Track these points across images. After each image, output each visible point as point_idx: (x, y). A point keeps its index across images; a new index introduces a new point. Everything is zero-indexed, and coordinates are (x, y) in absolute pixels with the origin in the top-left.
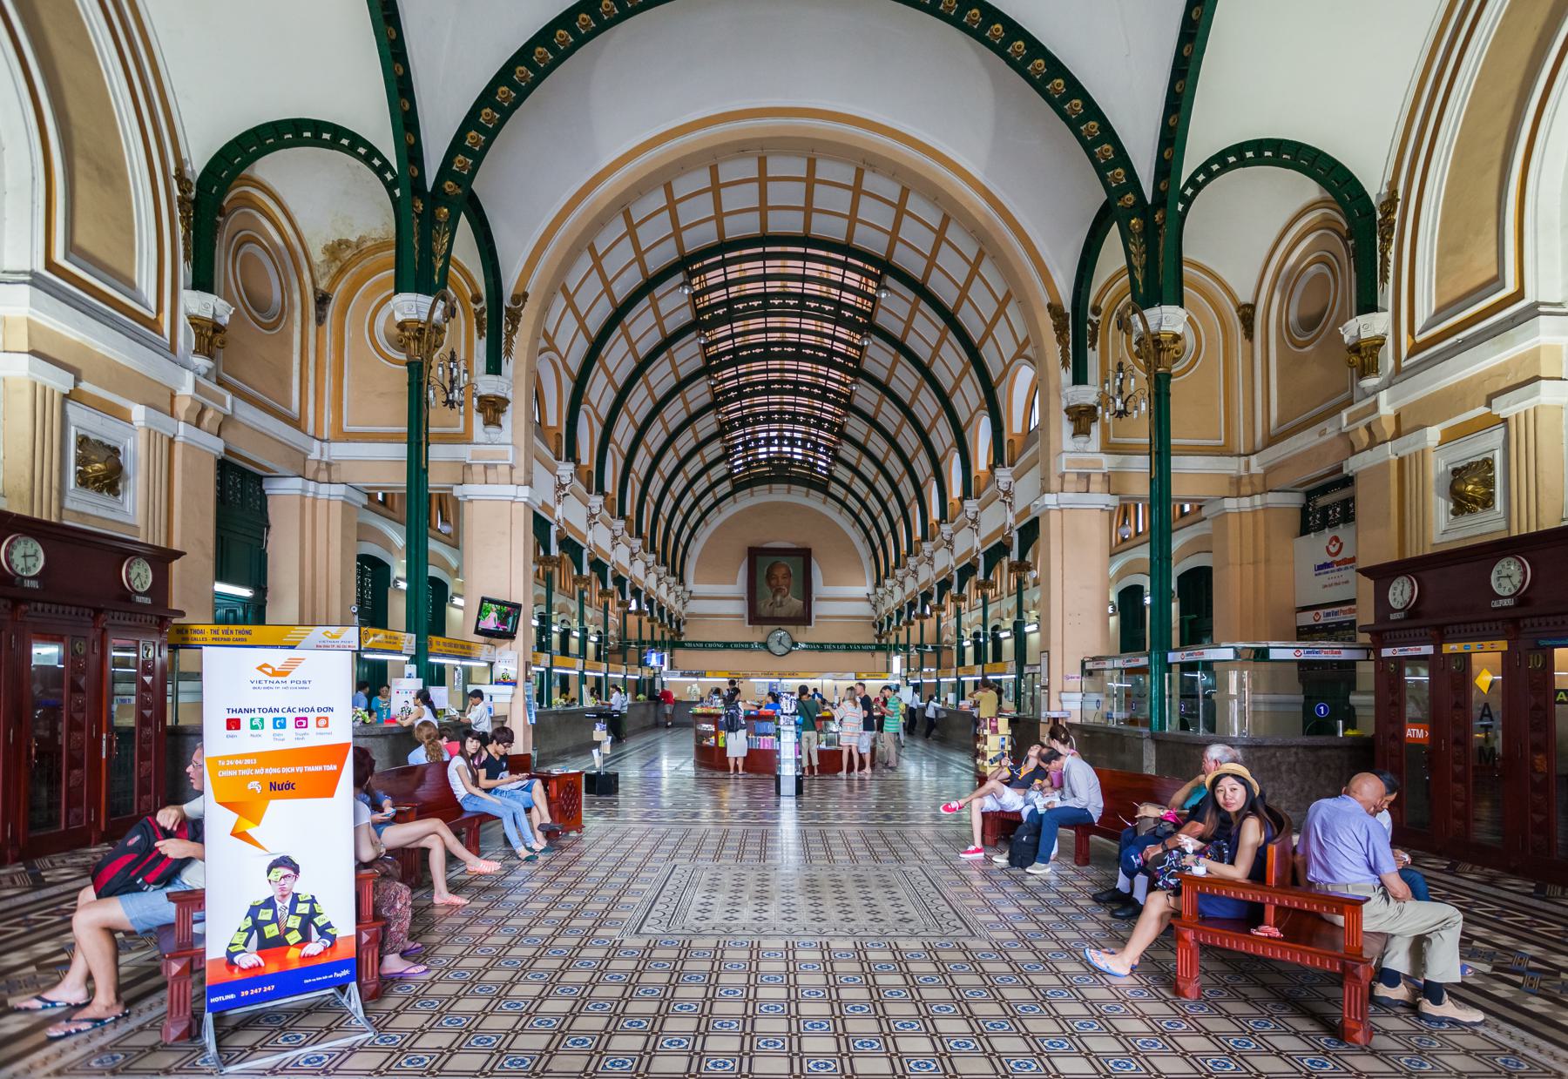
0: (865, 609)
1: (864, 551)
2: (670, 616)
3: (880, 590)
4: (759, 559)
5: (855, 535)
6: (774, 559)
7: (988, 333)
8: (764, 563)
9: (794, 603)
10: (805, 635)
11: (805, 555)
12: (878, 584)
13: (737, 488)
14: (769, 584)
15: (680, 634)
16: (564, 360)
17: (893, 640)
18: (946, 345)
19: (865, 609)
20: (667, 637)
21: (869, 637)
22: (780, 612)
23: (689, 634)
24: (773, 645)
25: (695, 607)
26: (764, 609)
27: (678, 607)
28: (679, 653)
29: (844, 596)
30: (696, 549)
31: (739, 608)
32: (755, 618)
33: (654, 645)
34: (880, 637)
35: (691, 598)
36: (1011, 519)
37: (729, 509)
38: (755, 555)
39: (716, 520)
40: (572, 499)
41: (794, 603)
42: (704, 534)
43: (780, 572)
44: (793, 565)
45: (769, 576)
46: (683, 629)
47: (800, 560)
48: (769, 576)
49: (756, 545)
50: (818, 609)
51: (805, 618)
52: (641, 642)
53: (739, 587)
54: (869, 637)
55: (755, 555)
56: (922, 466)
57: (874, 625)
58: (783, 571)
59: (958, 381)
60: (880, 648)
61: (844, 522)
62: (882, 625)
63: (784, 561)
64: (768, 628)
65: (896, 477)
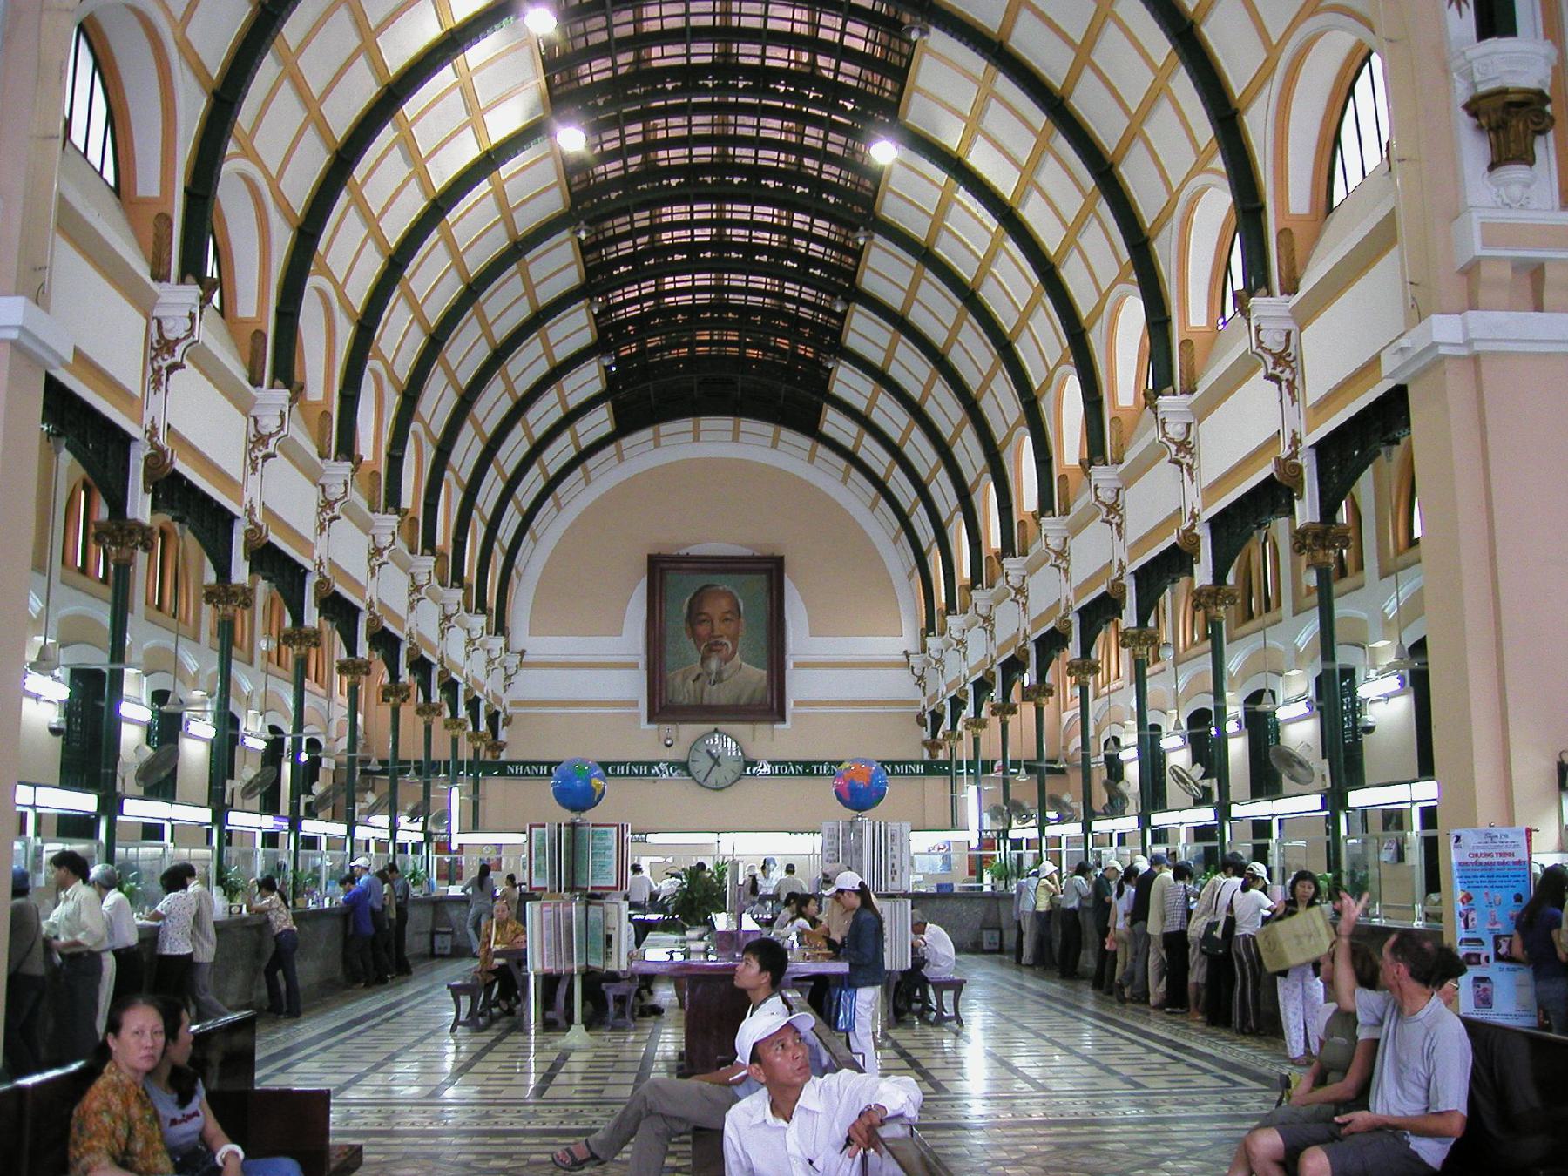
0: (900, 685)
1: (898, 560)
2: (473, 704)
3: (932, 642)
4: (672, 577)
5: (879, 527)
6: (702, 580)
7: (1133, 134)
8: (682, 588)
9: (750, 675)
10: (770, 742)
11: (771, 569)
12: (929, 628)
13: (625, 424)
14: (694, 634)
15: (497, 747)
16: (274, 183)
17: (964, 752)
18: (1050, 164)
19: (900, 685)
20: (466, 753)
21: (911, 746)
22: (719, 695)
23: (517, 745)
24: (701, 765)
25: (531, 685)
26: (683, 689)
27: (491, 688)
28: (494, 787)
29: (854, 662)
30: (534, 560)
31: (633, 685)
32: (662, 708)
33: (453, 769)
34: (933, 745)
35: (521, 665)
36: (1193, 499)
37: (608, 473)
38: (661, 569)
39: (578, 496)
40: (280, 464)
41: (750, 675)
42: (552, 527)
43: (716, 608)
44: (748, 591)
45: (694, 616)
46: (503, 735)
47: (759, 582)
48: (694, 616)
49: (664, 552)
50: (799, 686)
51: (772, 707)
52: (427, 768)
53: (631, 639)
54: (911, 746)
55: (661, 569)
56: (1002, 405)
57: (921, 720)
58: (724, 605)
59: (1074, 231)
60: (932, 768)
61: (854, 497)
62: (937, 718)
63: (725, 583)
64: (688, 732)
65: (947, 432)
